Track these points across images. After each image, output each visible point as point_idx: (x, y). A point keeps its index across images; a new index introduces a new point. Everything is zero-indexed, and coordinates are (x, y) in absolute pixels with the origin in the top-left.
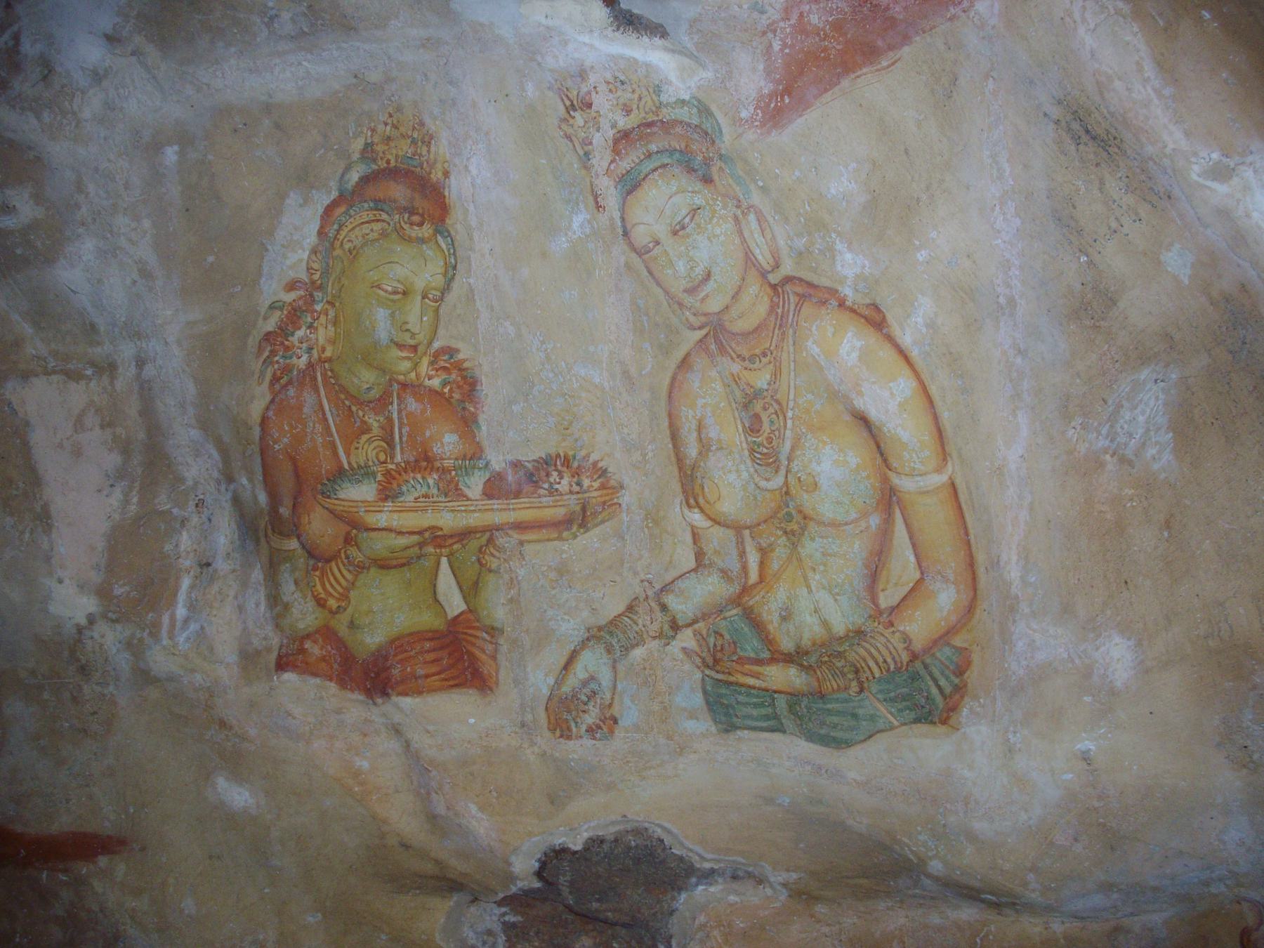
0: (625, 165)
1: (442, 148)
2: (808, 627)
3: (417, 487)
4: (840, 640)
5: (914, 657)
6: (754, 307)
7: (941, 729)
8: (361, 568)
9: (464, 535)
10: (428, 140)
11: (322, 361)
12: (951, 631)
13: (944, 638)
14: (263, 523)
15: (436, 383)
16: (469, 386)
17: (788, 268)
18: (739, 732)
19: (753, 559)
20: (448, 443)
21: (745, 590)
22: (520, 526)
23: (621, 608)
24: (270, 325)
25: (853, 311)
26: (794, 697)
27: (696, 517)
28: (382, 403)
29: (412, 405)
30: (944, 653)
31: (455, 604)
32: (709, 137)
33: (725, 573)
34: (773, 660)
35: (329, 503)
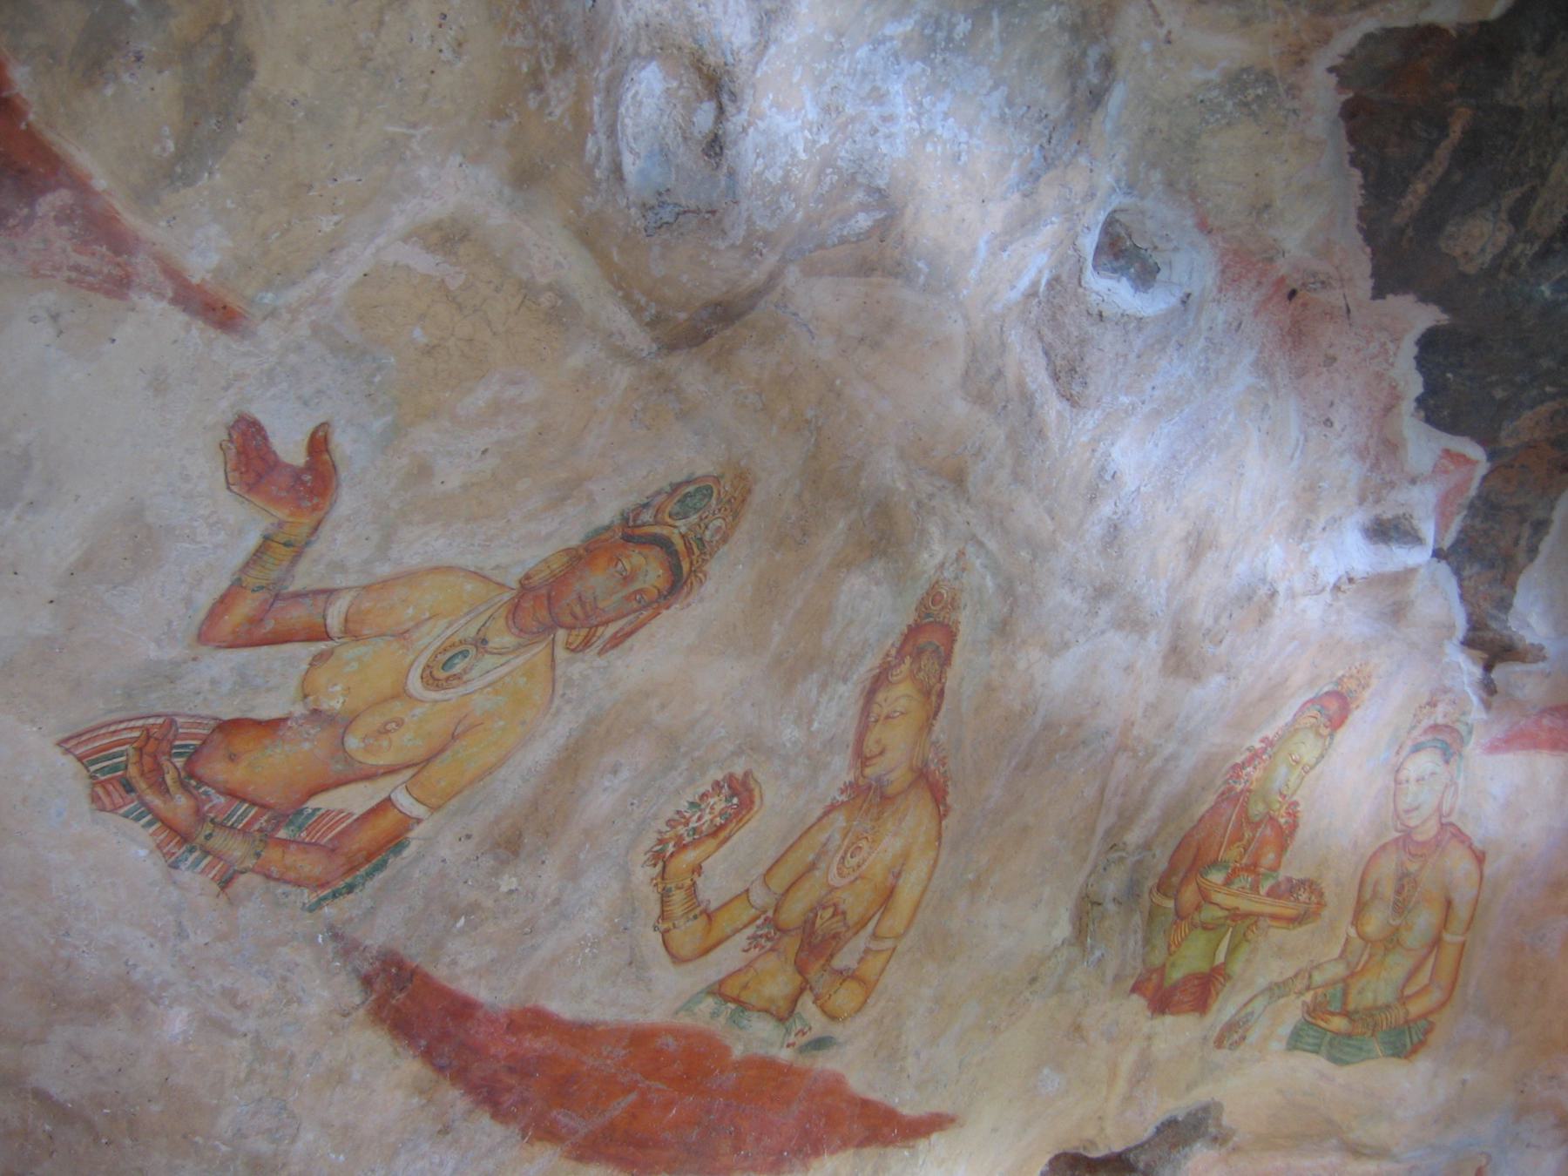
0: (1423, 739)
1: (1366, 694)
2: (1368, 999)
3: (1245, 880)
4: (1377, 1008)
5: (1407, 1022)
6: (1429, 831)
7: (1403, 1061)
8: (1194, 926)
9: (1247, 915)
10: (1365, 686)
11: (1249, 791)
12: (1431, 1012)
13: (1424, 1016)
14: (1151, 882)
15: (1282, 821)
16: (1294, 826)
17: (1454, 819)
18: (1297, 1052)
19: (1365, 958)
20: (1269, 858)
21: (1352, 975)
22: (1274, 917)
23: (1290, 973)
24: (1239, 760)
25: (1473, 851)
26: (1337, 1034)
27: (1352, 932)
28: (1258, 824)
29: (1268, 831)
30: (1422, 1024)
31: (1220, 958)
32: (1462, 742)
33: (1348, 964)
34: (1340, 1014)
35: (1200, 880)
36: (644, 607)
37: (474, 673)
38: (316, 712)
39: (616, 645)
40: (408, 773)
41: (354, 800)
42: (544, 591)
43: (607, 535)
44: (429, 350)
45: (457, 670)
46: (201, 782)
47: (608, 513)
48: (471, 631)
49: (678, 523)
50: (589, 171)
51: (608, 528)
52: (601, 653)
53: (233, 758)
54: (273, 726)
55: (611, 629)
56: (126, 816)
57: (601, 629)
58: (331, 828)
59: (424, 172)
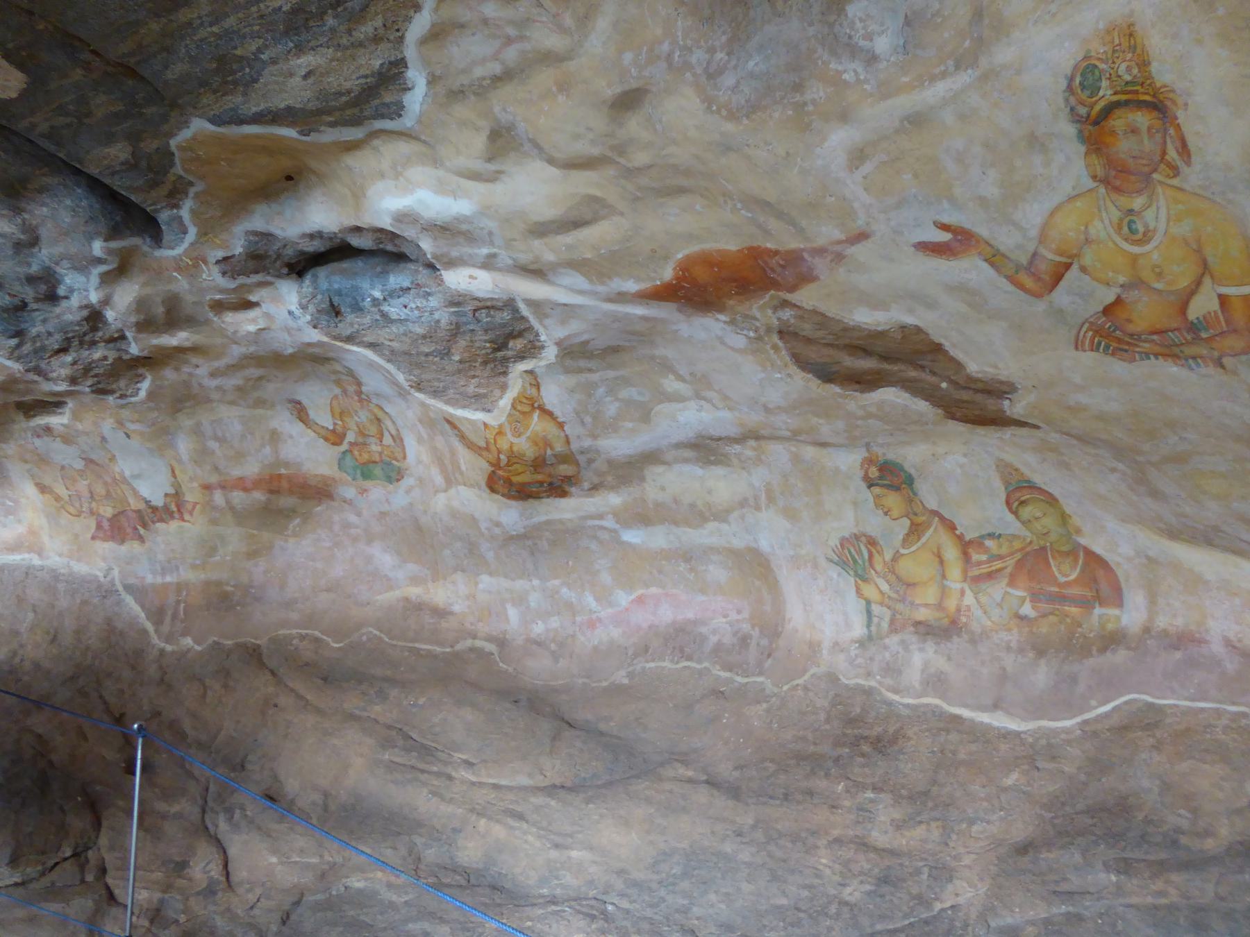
36: (1165, 130)
37: (1152, 225)
38: (1122, 286)
39: (1189, 156)
40: (1207, 281)
41: (1203, 305)
42: (1113, 173)
43: (1086, 134)
44: (916, 176)
45: (1141, 229)
46: (1139, 335)
47: (1070, 130)
48: (1116, 214)
49: (1101, 93)
50: (858, 80)
51: (1080, 132)
52: (1188, 164)
53: (1129, 321)
54: (1118, 301)
55: (1172, 154)
56: (1142, 359)
57: (1167, 157)
58: (1219, 322)
59: (819, 162)
